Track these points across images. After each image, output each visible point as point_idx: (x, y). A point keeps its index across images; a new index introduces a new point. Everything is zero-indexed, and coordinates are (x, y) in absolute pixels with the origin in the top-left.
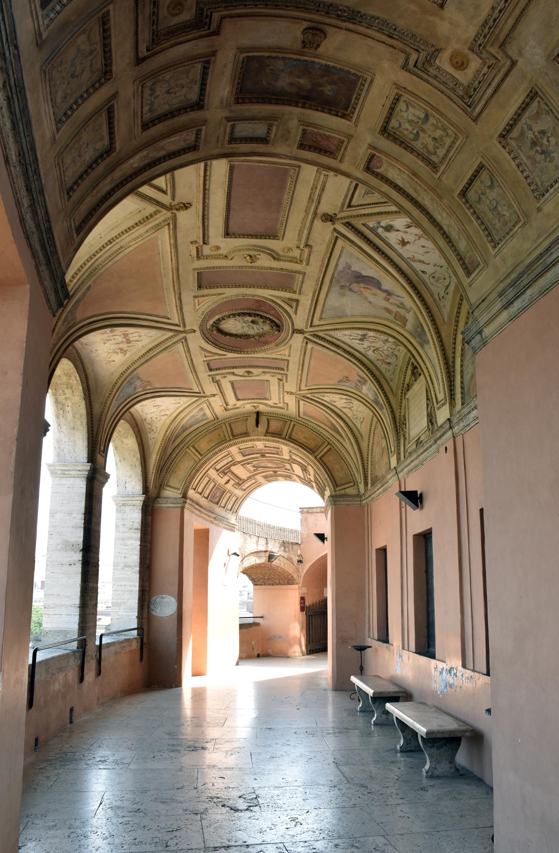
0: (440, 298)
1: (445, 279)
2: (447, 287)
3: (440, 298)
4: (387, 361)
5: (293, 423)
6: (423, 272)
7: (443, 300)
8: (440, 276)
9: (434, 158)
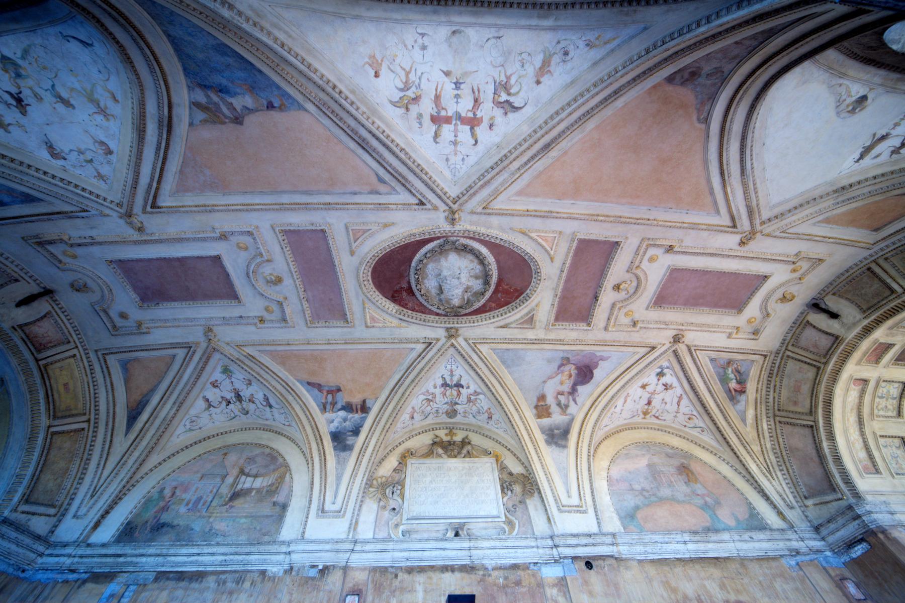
4: (415, 415)
5: (75, 351)
9: (876, 411)
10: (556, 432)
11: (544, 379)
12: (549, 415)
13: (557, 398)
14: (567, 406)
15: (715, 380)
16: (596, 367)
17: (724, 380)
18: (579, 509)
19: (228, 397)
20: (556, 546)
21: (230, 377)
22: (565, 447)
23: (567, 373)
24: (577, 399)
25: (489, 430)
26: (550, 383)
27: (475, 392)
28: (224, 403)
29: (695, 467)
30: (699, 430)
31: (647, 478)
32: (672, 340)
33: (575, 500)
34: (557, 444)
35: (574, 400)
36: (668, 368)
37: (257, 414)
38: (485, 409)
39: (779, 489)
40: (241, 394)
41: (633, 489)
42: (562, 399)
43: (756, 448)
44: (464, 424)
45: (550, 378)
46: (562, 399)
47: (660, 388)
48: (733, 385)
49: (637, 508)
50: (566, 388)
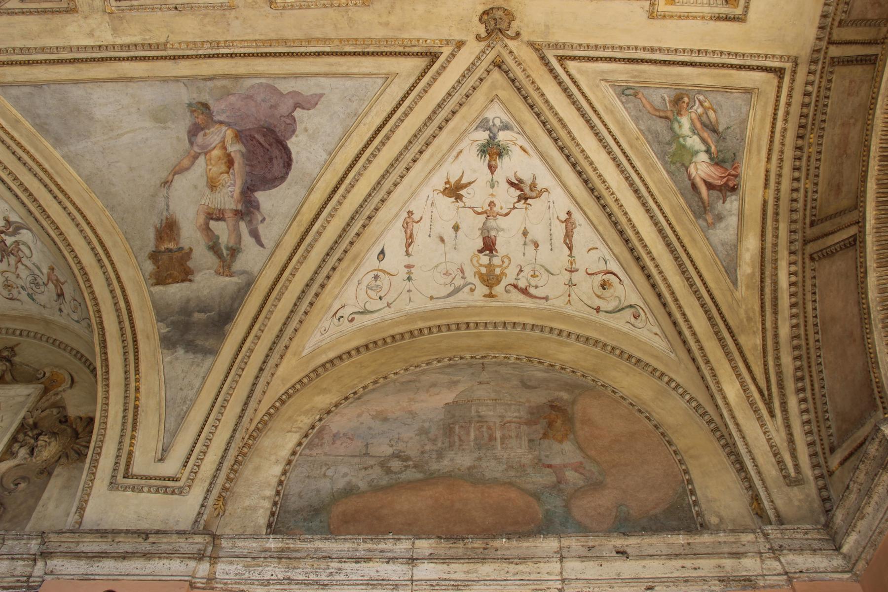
0: (336, 313)
1: (380, 298)
2: (365, 312)
3: (336, 313)
6: (382, 252)
7: (336, 320)
8: (386, 287)
10: (197, 316)
11: (164, 175)
12: (186, 275)
13: (207, 229)
14: (234, 251)
15: (644, 158)
16: (291, 126)
17: (676, 158)
18: (168, 486)
20: (46, 555)
22: (213, 352)
23: (216, 153)
24: (262, 229)
25: (65, 329)
26: (182, 183)
27: (8, 222)
29: (589, 408)
30: (628, 313)
31: (423, 432)
32: (482, 30)
33: (170, 467)
34: (191, 347)
35: (255, 234)
36: (506, 127)
38: (45, 270)
39: (780, 438)
41: (366, 454)
42: (221, 229)
43: (751, 342)
44: (14, 318)
45: (178, 170)
46: (221, 229)
47: (506, 196)
48: (702, 168)
49: (349, 491)
50: (228, 196)
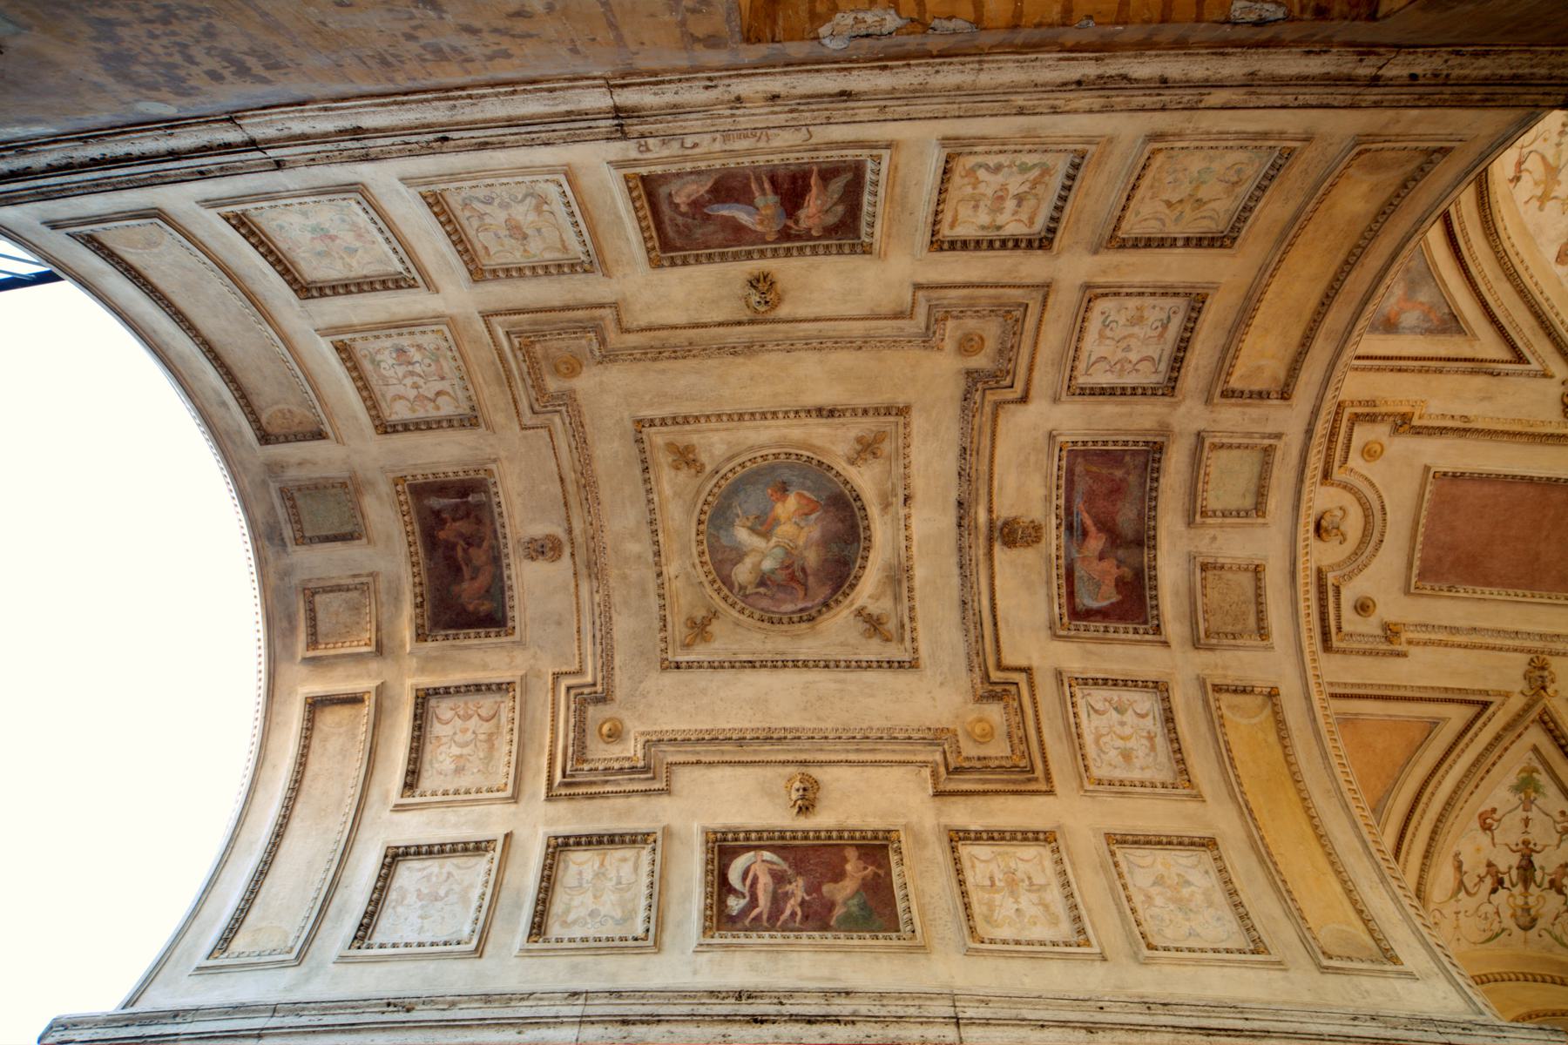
19: (1502, 867)
21: (1528, 804)
28: (1489, 882)
37: (1558, 930)
40: (1536, 859)
